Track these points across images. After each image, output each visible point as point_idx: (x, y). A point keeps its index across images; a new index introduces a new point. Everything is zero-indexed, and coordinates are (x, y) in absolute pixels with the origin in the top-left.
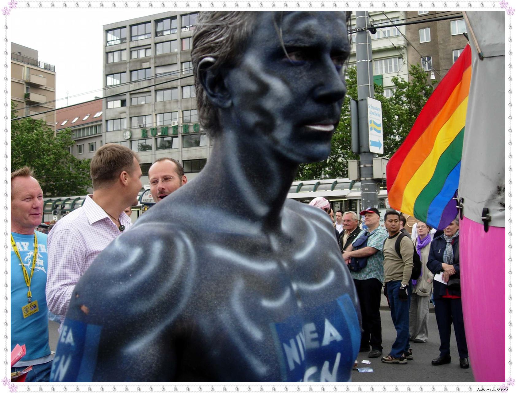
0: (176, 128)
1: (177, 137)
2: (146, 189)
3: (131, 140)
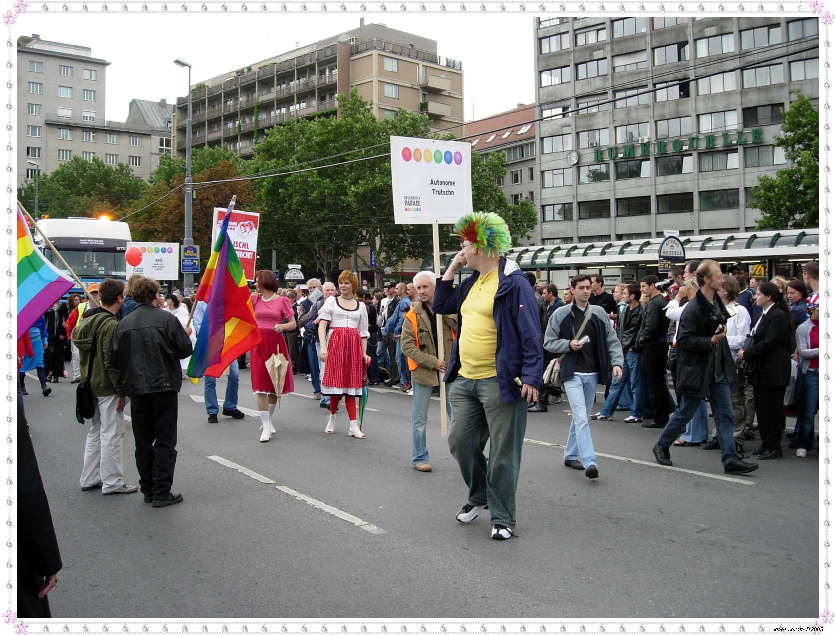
0: (646, 146)
1: (648, 160)
2: (666, 235)
3: (578, 166)
